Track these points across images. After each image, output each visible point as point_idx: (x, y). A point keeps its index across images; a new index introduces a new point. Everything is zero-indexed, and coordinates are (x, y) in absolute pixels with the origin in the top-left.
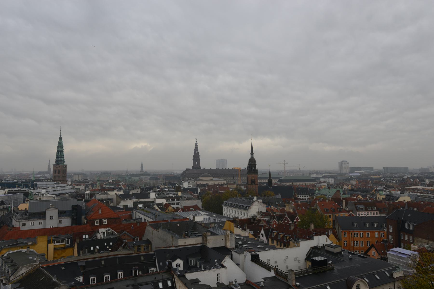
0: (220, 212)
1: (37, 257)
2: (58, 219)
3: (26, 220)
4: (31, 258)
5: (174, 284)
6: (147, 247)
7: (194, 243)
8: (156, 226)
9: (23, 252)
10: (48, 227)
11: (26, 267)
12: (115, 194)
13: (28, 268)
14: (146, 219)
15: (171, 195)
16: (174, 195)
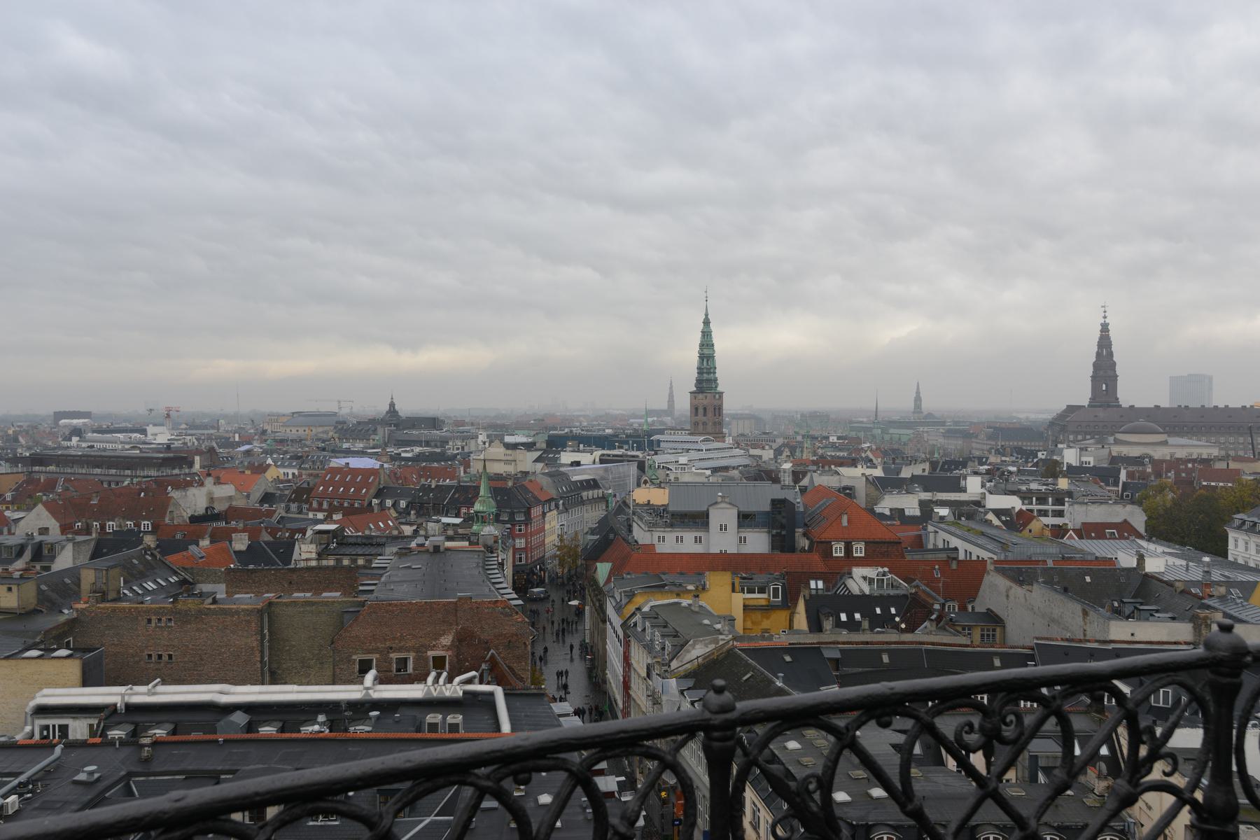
0: (1219, 548)
1: (722, 622)
2: (738, 532)
3: (666, 529)
4: (706, 622)
5: (1118, 751)
6: (989, 631)
7: (1165, 639)
8: (1021, 573)
9: (683, 605)
11: (703, 642)
12: (860, 475)
13: (707, 647)
14: (970, 553)
15: (1034, 486)
16: (1045, 487)
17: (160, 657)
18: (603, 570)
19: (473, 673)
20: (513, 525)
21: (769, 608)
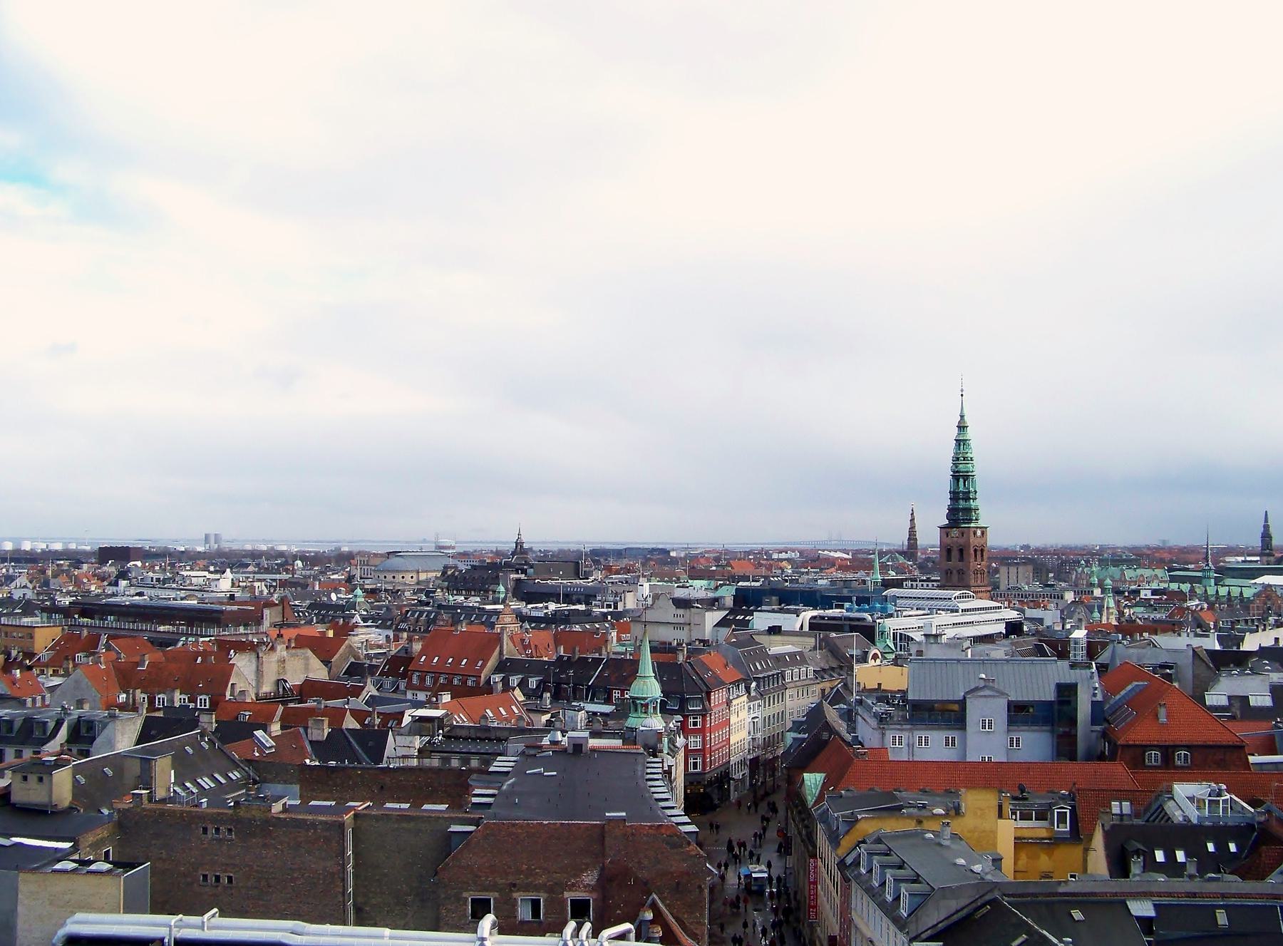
2: (1008, 731)
3: (904, 727)
4: (961, 861)
10: (973, 757)
17: (218, 878)
18: (813, 780)
19: (627, 926)
20: (686, 717)
21: (1055, 842)
